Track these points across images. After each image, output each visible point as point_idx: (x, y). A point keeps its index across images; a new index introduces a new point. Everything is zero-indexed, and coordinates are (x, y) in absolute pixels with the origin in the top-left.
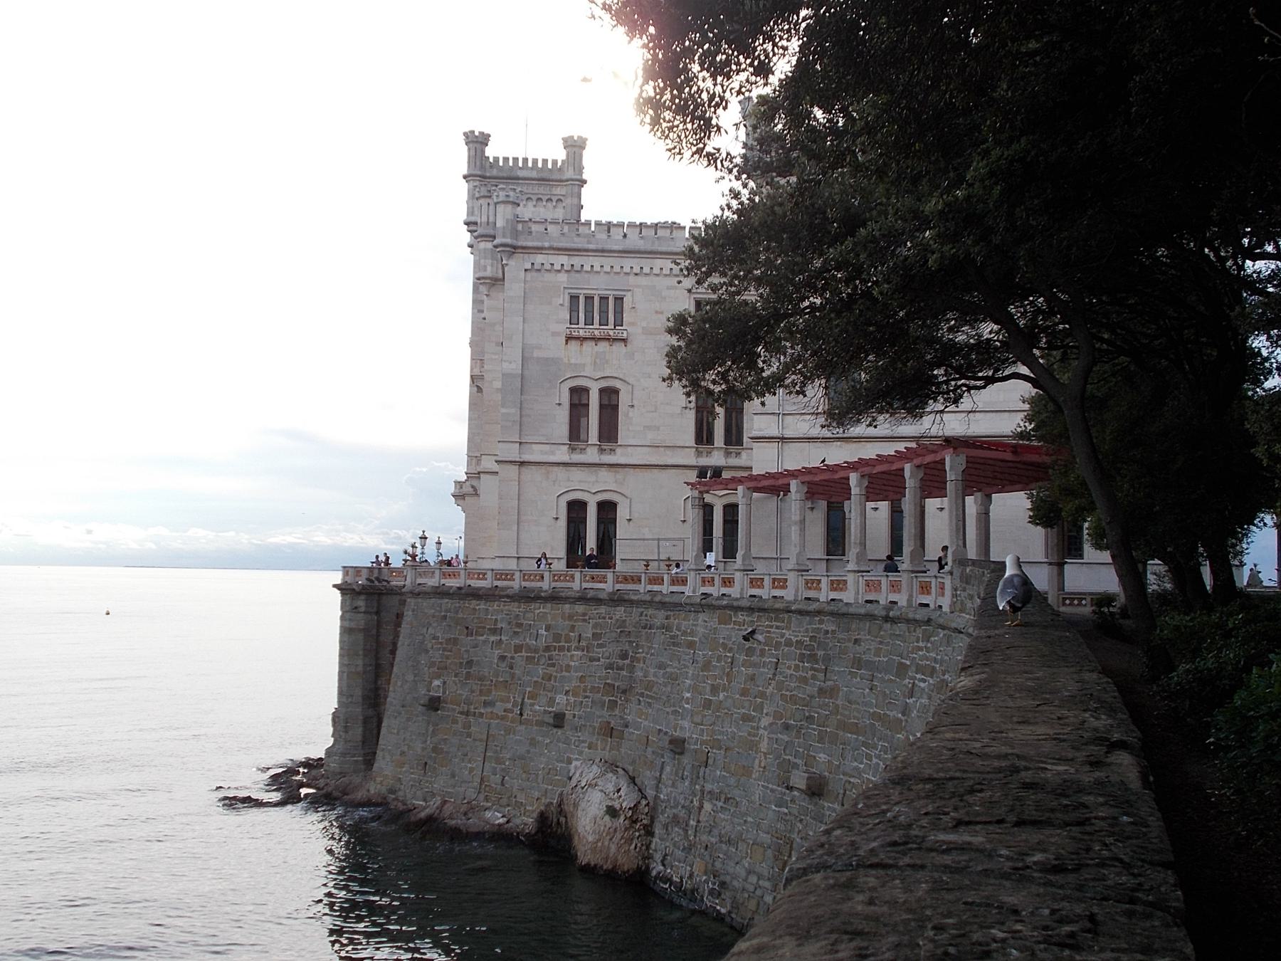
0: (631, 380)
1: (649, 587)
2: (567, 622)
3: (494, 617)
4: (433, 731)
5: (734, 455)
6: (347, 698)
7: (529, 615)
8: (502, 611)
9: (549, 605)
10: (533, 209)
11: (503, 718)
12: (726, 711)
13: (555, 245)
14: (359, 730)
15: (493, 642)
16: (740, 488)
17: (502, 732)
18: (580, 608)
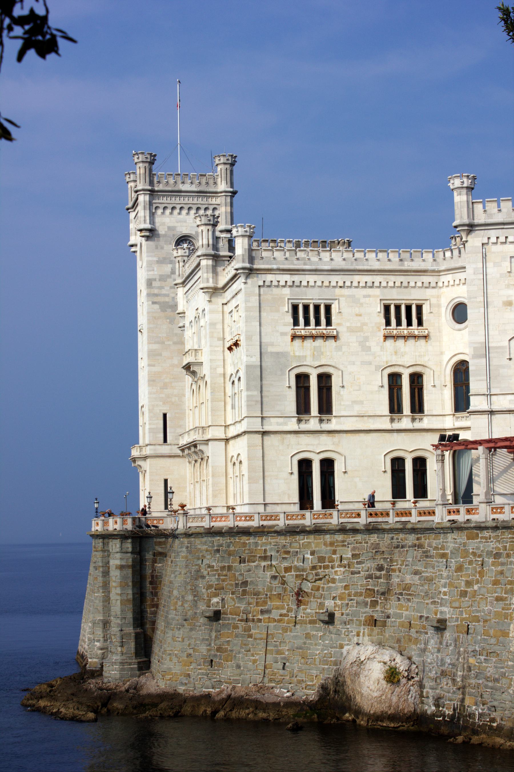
0: (341, 367)
1: (397, 519)
2: (329, 548)
3: (263, 548)
4: (216, 637)
6: (121, 620)
7: (295, 545)
8: (271, 543)
9: (312, 537)
11: (279, 621)
12: (481, 596)
13: (282, 267)
14: (132, 645)
15: (264, 566)
16: (481, 448)
17: (280, 631)
18: (339, 537)
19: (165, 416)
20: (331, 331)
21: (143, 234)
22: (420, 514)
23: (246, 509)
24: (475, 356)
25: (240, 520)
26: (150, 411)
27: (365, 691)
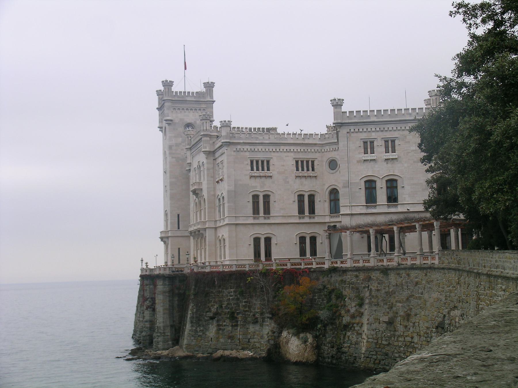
5: (312, 218)
10: (193, 114)
13: (245, 141)
16: (348, 232)
19: (178, 215)
20: (268, 173)
21: (167, 122)
22: (317, 264)
23: (227, 263)
24: (344, 187)
25: (226, 268)
26: (171, 213)
27: (291, 351)
